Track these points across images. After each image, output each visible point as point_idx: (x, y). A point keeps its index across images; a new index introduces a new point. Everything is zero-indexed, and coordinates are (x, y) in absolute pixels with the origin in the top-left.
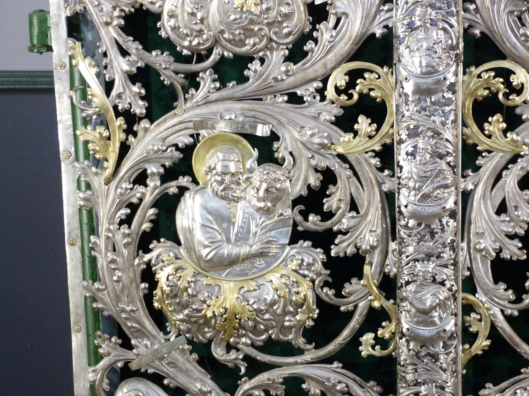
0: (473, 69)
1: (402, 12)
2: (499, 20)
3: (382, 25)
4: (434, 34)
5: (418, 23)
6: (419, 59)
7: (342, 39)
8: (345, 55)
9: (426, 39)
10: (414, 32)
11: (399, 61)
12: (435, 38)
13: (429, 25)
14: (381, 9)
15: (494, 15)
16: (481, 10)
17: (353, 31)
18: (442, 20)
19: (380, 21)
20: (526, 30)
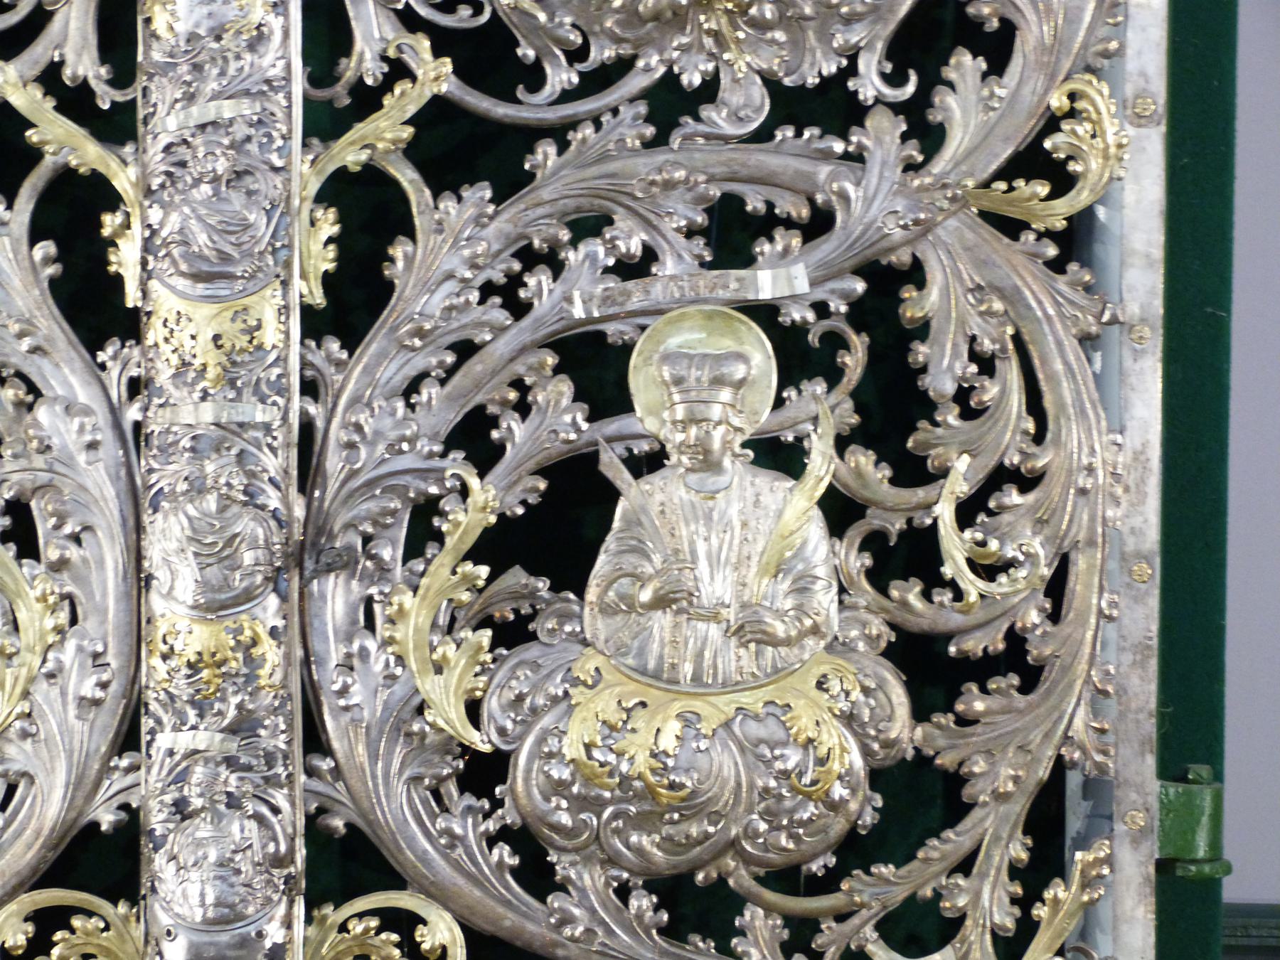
0: (328, 909)
1: (159, 773)
2: (387, 796)
3: (116, 802)
4: (235, 828)
5: (197, 803)
6: (198, 886)
7: (18, 834)
8: (25, 873)
9: (216, 840)
10: (187, 822)
11: (153, 890)
12: (238, 837)
13: (222, 807)
14: (112, 764)
15: (376, 785)
16: (347, 775)
17: (45, 818)
18: (255, 796)
19: (111, 792)
20: (451, 822)
